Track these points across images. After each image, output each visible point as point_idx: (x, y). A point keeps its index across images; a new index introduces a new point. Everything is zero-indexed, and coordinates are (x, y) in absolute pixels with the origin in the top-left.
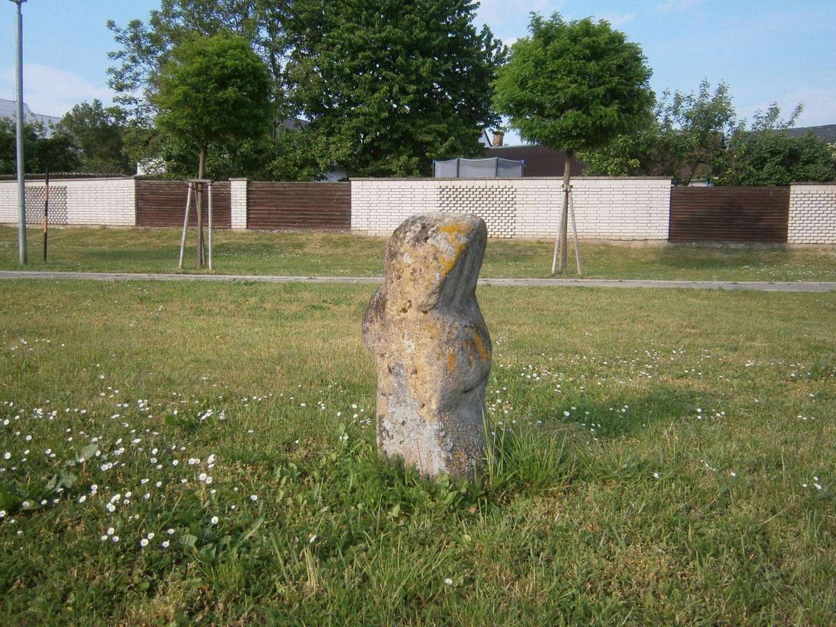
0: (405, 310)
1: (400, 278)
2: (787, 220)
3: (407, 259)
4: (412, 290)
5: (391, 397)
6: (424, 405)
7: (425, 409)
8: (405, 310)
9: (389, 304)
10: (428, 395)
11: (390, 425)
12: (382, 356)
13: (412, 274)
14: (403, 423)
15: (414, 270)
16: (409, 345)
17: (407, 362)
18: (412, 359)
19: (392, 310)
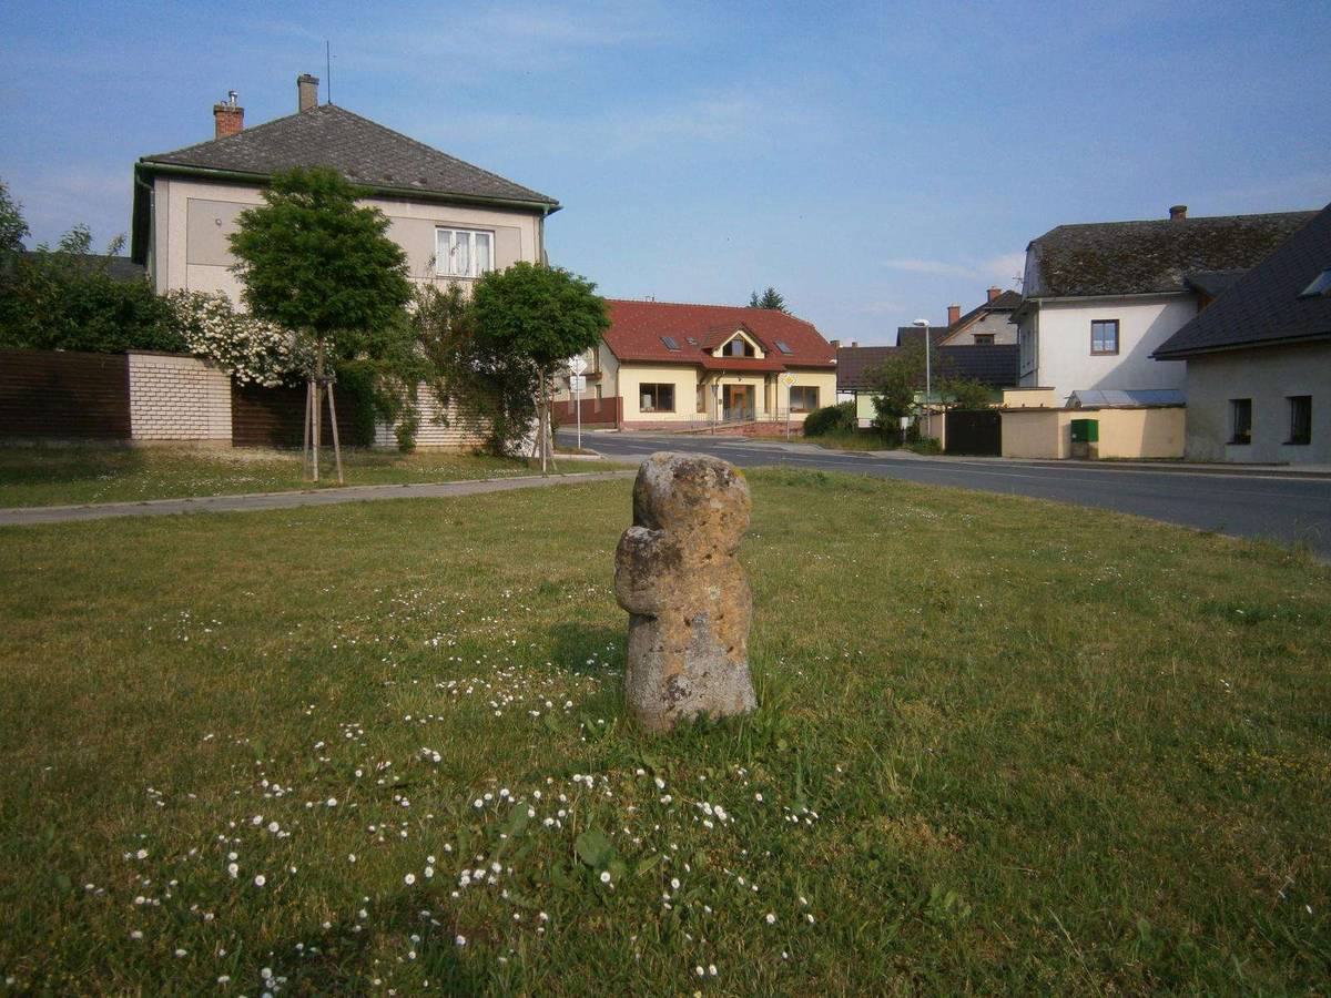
0: (709, 557)
1: (704, 523)
2: (127, 404)
3: (716, 504)
4: (720, 534)
5: (687, 652)
6: (731, 649)
7: (735, 651)
8: (709, 557)
9: (686, 553)
10: (737, 636)
11: (687, 681)
12: (677, 609)
13: (722, 519)
14: (705, 675)
15: (724, 515)
16: (712, 591)
17: (711, 610)
18: (717, 604)
19: (691, 559)
